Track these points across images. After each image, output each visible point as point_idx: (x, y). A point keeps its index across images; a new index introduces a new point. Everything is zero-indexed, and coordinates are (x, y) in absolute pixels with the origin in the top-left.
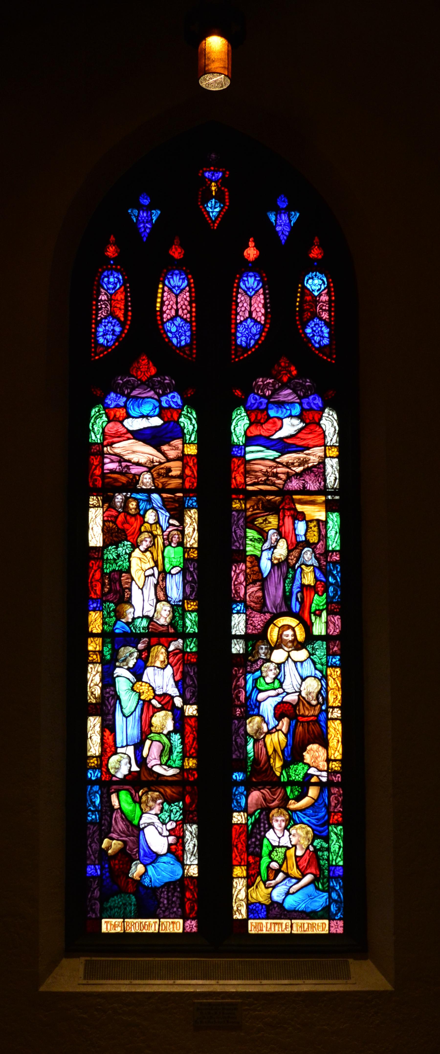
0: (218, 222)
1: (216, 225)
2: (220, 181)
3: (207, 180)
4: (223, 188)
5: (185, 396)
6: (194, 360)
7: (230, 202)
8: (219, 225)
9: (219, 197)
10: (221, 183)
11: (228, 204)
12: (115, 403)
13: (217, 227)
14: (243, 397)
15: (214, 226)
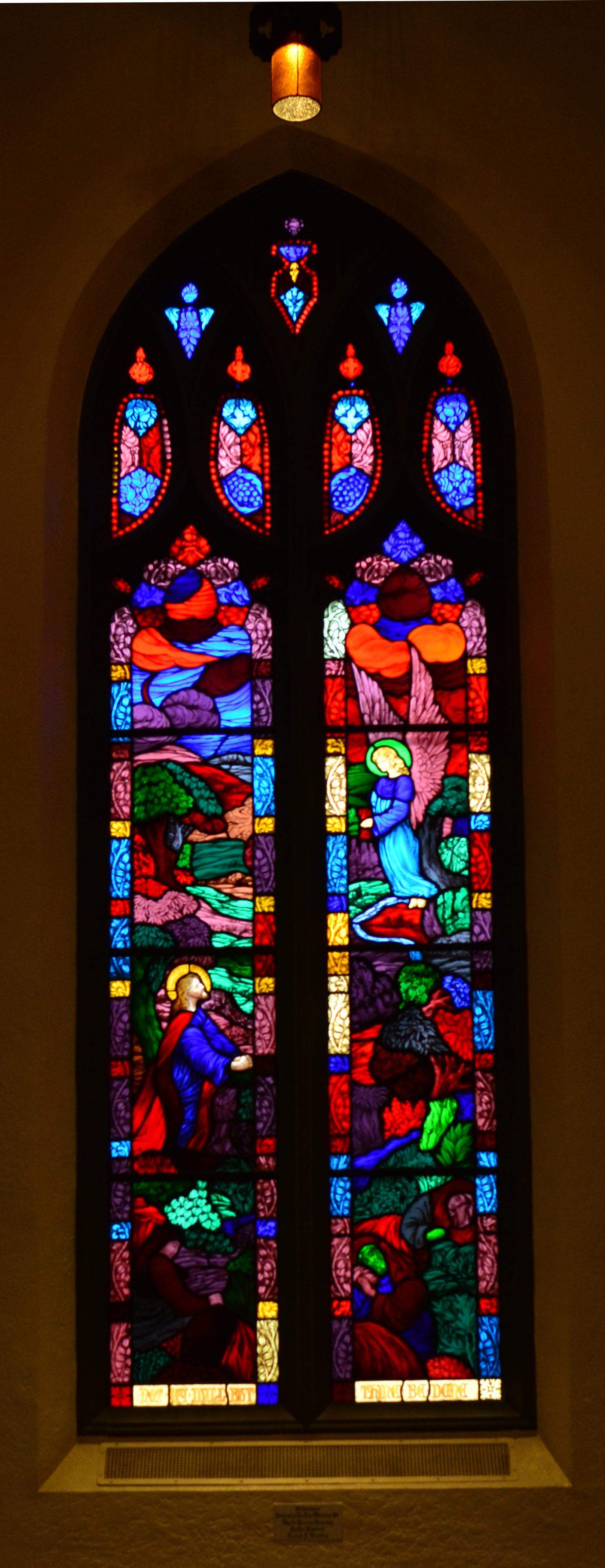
0: (301, 321)
1: (298, 326)
2: (306, 259)
3: (284, 260)
4: (308, 271)
5: (254, 587)
6: (268, 534)
7: (319, 291)
8: (303, 326)
9: (303, 284)
10: (306, 263)
11: (316, 294)
12: (148, 600)
13: (301, 330)
14: (342, 587)
15: (295, 328)
